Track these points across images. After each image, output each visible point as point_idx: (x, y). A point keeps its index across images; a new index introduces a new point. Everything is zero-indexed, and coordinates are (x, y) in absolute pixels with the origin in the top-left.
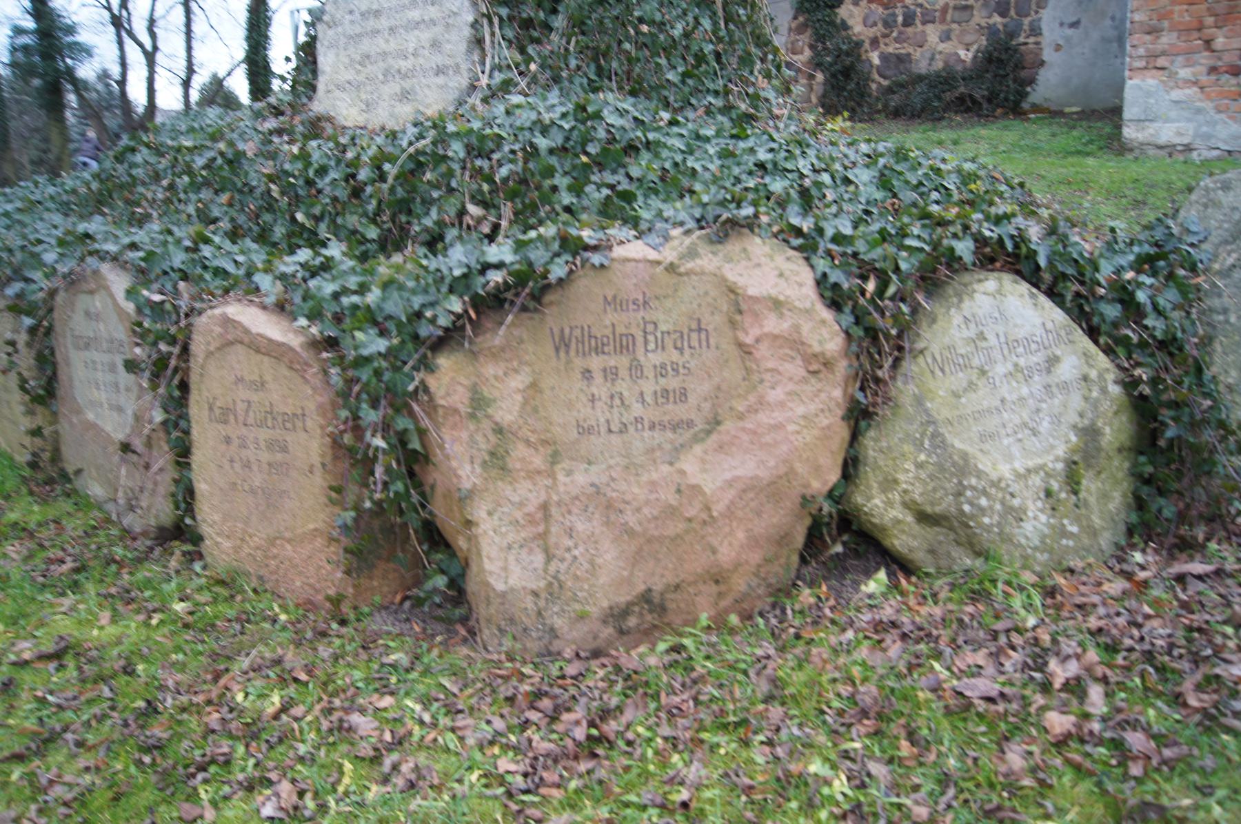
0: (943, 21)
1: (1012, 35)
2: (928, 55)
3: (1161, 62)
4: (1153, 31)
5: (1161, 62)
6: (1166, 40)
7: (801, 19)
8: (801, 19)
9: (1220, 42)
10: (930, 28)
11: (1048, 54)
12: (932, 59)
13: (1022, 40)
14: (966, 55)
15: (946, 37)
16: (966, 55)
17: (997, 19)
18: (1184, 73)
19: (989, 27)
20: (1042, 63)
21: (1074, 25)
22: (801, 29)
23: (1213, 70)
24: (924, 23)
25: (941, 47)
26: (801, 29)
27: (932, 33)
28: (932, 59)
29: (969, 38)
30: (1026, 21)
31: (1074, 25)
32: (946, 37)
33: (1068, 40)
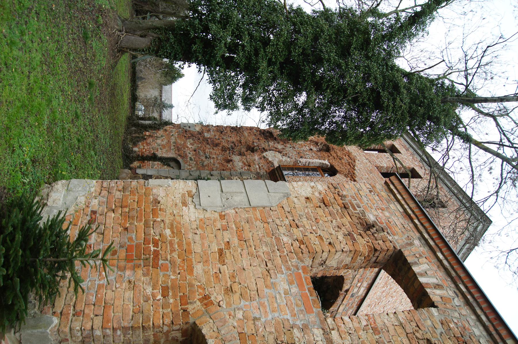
3: (104, 193)
4: (124, 189)
6: (118, 195)
18: (95, 203)
23: (94, 212)
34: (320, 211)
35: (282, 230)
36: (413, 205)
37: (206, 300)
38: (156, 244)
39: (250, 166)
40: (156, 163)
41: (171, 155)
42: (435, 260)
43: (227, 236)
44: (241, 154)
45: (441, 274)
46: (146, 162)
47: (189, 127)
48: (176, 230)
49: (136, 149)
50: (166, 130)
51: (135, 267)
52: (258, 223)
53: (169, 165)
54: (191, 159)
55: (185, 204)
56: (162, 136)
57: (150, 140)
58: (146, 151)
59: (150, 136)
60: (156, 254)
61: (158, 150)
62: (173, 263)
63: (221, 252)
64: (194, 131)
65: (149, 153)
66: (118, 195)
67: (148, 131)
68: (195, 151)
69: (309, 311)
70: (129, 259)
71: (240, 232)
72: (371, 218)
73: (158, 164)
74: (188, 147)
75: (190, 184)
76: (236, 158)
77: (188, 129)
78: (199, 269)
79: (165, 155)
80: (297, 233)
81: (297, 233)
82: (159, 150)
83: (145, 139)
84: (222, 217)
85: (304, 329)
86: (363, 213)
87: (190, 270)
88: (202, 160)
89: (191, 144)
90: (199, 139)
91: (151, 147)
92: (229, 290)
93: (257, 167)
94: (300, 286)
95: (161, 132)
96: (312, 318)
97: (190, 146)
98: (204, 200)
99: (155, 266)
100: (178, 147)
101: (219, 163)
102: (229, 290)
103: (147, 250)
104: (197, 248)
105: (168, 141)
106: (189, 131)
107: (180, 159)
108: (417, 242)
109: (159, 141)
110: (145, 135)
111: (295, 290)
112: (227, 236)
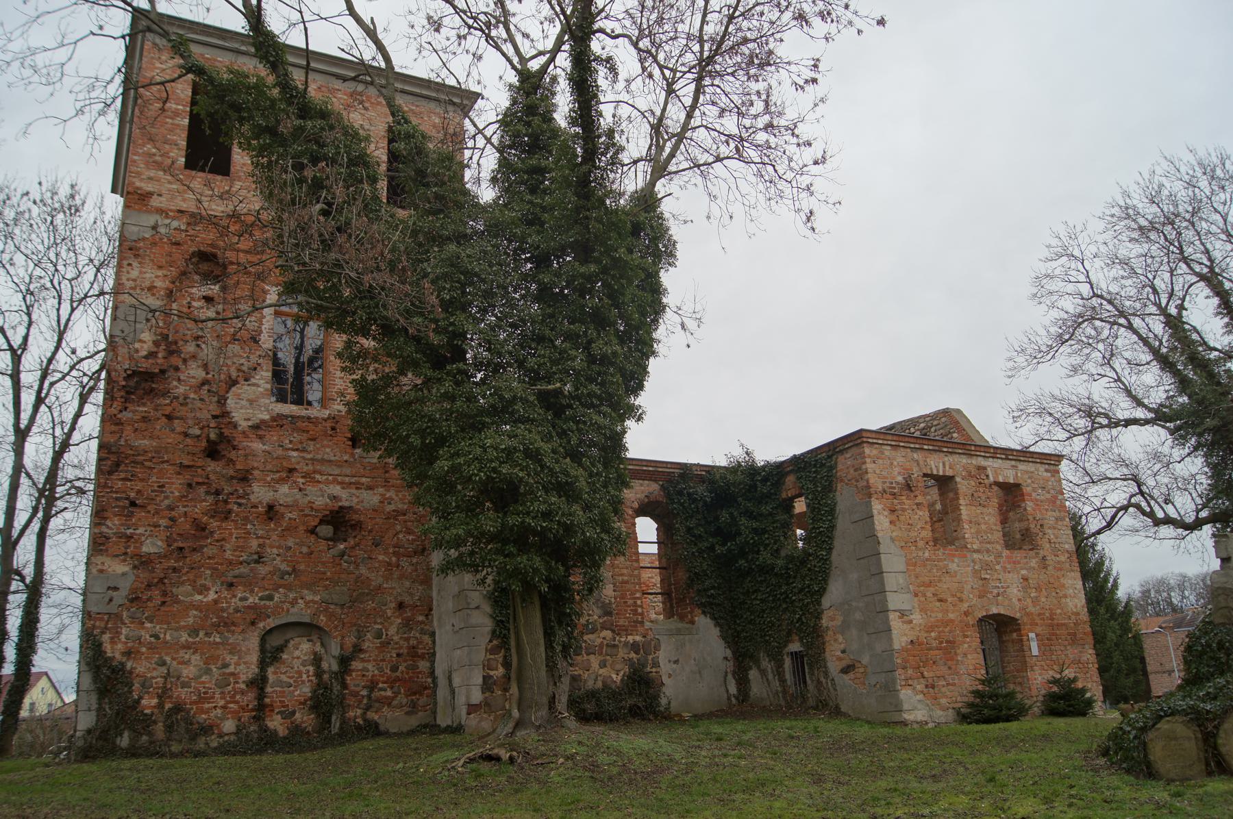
0: (600, 654)
1: (644, 666)
2: (593, 677)
4: (904, 668)
5: (910, 682)
6: (910, 672)
7: (495, 642)
8: (495, 642)
9: (925, 673)
10: (592, 657)
11: (665, 679)
12: (596, 680)
13: (649, 669)
14: (617, 678)
15: (603, 665)
16: (617, 678)
17: (633, 655)
18: (919, 687)
19: (630, 660)
20: (663, 684)
21: (676, 662)
22: (493, 651)
23: (927, 686)
24: (588, 654)
25: (601, 671)
26: (493, 651)
27: (594, 661)
28: (596, 680)
29: (618, 667)
30: (650, 657)
31: (676, 662)
32: (603, 665)
33: (674, 671)
34: (902, 518)
35: (920, 554)
36: (890, 437)
37: (966, 614)
38: (941, 643)
39: (291, 471)
40: (271, 678)
41: (253, 642)
42: (927, 454)
43: (929, 594)
44: (244, 478)
45: (936, 456)
46: (267, 700)
47: (116, 589)
48: (929, 629)
49: (229, 726)
50: (128, 653)
51: (956, 654)
52: (918, 570)
53: (281, 649)
54: (270, 598)
55: (910, 622)
56: (164, 664)
57: (182, 694)
58: (237, 702)
59: (163, 695)
60: (947, 642)
61: (233, 674)
62: (950, 632)
63: (940, 600)
64: (132, 578)
65: (243, 693)
66: (910, 672)
67: (138, 702)
68: (231, 585)
69: (965, 556)
70: (952, 660)
71: (924, 584)
72: (900, 479)
73: (275, 673)
74: (216, 602)
75: (892, 616)
76: (260, 493)
77: (124, 592)
78: (951, 616)
79: (254, 658)
80: (921, 544)
81: (921, 544)
82: (231, 669)
83: (178, 708)
84: (916, 595)
85: (973, 561)
86: (898, 483)
87: (952, 621)
88: (272, 573)
89: (203, 590)
90: (175, 570)
91: (218, 691)
92: (961, 600)
93: (295, 454)
94: (954, 556)
95: (140, 667)
96: (968, 554)
97: (212, 596)
98: (906, 607)
99: (954, 642)
100: (216, 626)
101: (282, 536)
102: (961, 600)
103: (946, 648)
104: (940, 615)
105: (187, 647)
106: (133, 590)
107: (271, 623)
108: (915, 456)
109: (188, 672)
110: (160, 705)
111: (956, 560)
112: (929, 594)
